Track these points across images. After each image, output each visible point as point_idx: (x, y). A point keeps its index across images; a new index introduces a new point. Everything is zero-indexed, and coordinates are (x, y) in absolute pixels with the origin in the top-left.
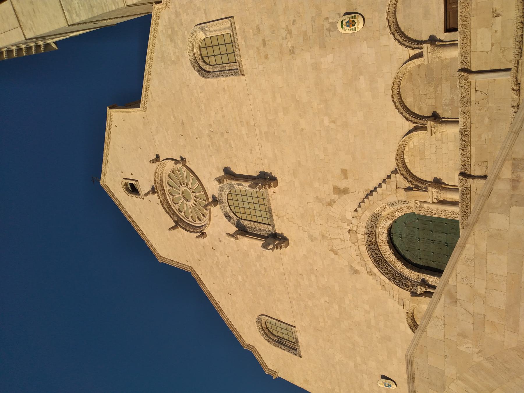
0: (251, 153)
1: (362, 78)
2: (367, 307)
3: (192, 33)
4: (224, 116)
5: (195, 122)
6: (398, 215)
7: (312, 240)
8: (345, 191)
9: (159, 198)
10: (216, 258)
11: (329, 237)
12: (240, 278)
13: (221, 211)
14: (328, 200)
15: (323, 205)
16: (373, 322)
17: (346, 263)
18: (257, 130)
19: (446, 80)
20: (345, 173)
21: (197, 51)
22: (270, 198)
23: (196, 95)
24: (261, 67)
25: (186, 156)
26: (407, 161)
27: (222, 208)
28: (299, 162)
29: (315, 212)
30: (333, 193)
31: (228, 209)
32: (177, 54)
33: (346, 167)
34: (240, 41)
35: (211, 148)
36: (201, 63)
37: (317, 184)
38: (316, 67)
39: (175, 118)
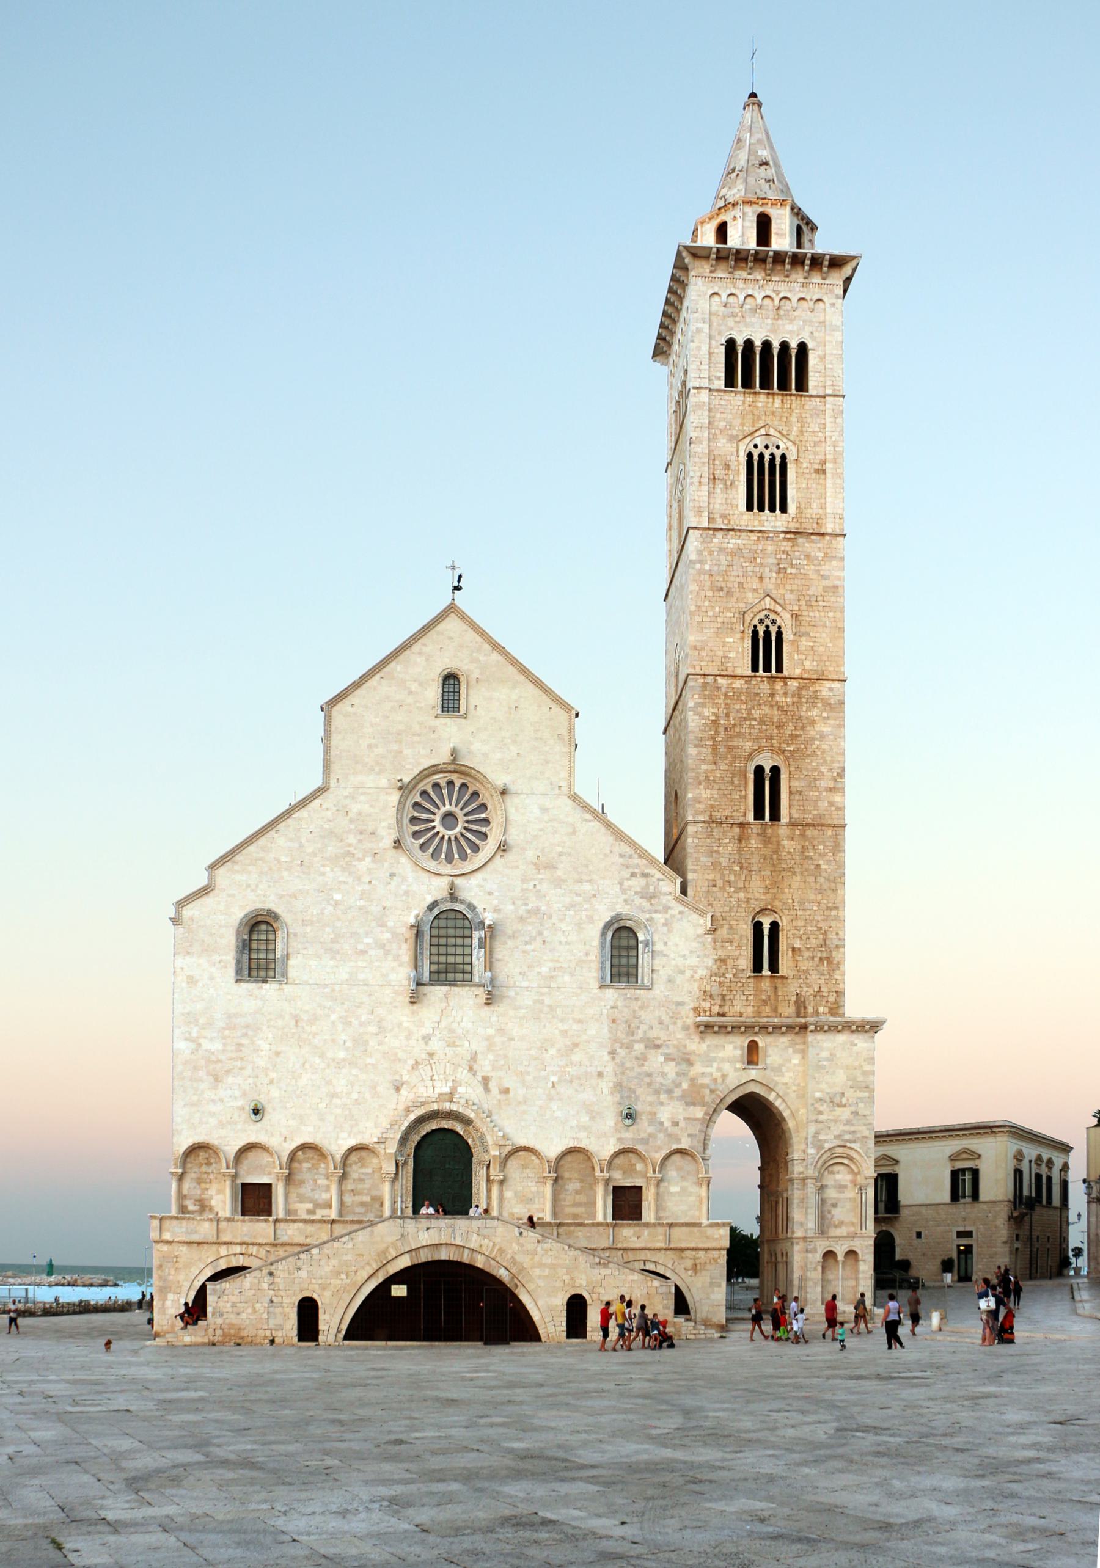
0: (520, 973)
1: (588, 1119)
2: (355, 1096)
3: (646, 927)
4: (560, 942)
5: (553, 891)
6: (470, 1141)
7: (424, 1038)
8: (487, 1089)
9: (444, 764)
10: (360, 856)
11: (432, 1061)
12: (337, 897)
13: (441, 897)
14: (475, 1067)
15: (468, 1061)
16: (336, 1101)
17: (405, 1078)
18: (546, 990)
19: (582, 1187)
20: (506, 1091)
21: (628, 924)
22: (467, 988)
23: (585, 906)
24: (605, 1011)
25: (510, 857)
26: (520, 1153)
27: (443, 900)
28: (513, 1039)
29: (459, 1049)
30: (483, 1074)
31: (443, 907)
32: (629, 892)
33: (511, 1095)
34: (630, 992)
35: (524, 907)
36: (616, 926)
37: (491, 1057)
38: (600, 1075)
39: (560, 854)
